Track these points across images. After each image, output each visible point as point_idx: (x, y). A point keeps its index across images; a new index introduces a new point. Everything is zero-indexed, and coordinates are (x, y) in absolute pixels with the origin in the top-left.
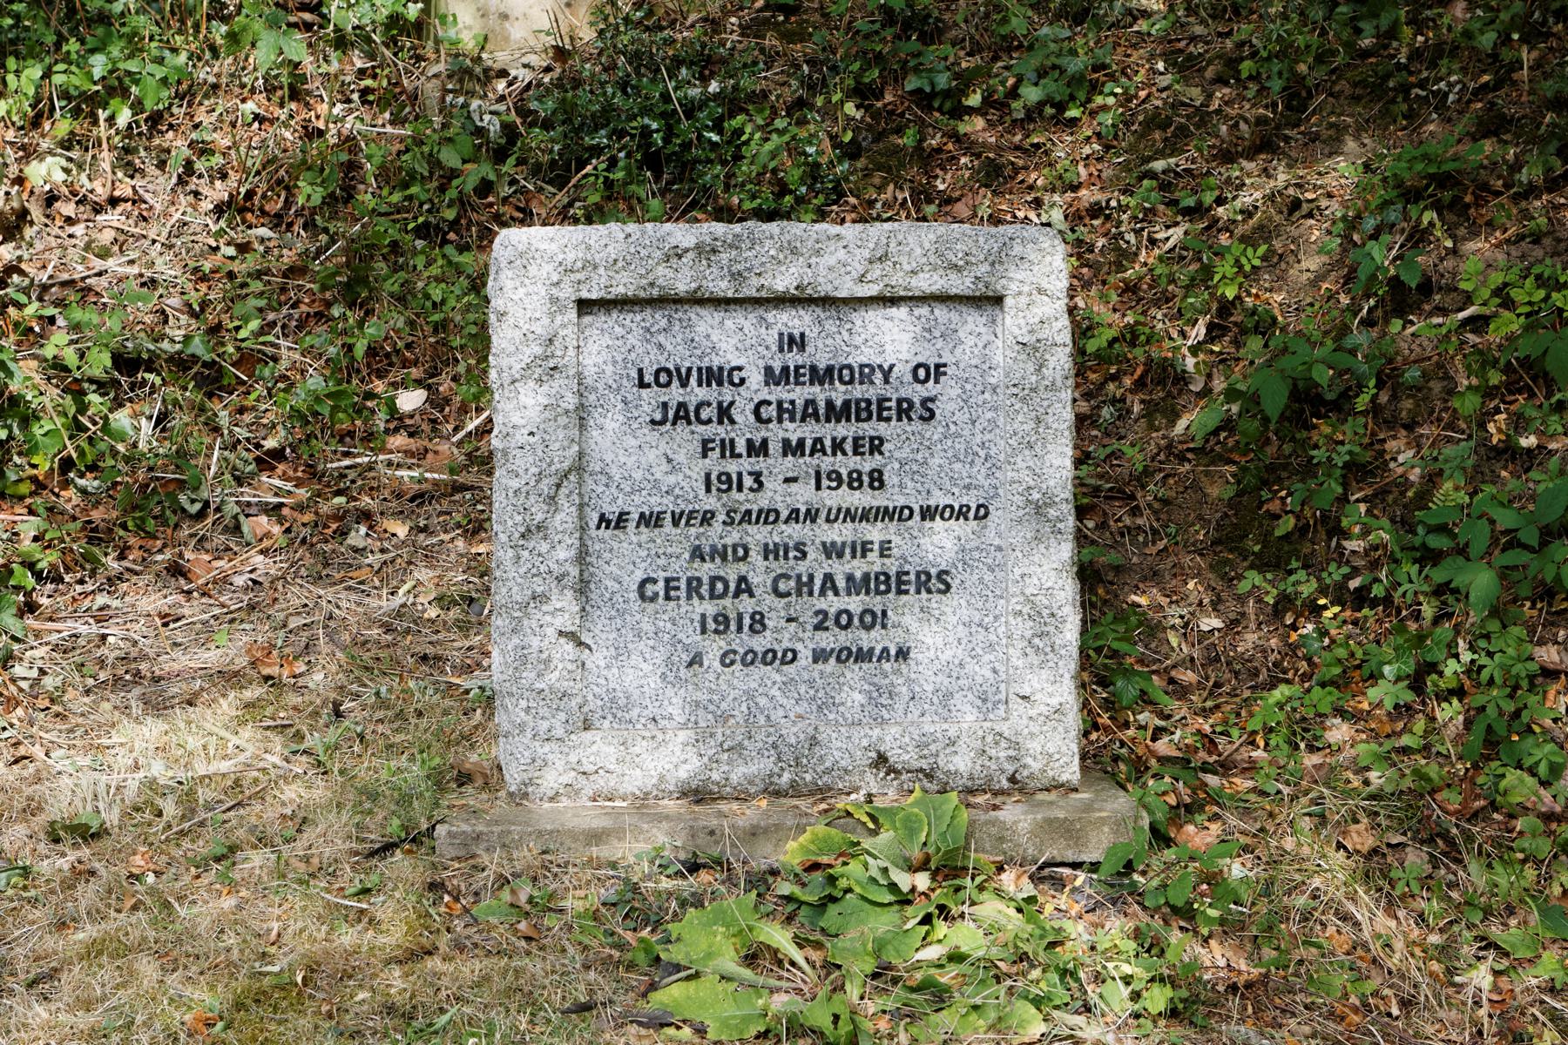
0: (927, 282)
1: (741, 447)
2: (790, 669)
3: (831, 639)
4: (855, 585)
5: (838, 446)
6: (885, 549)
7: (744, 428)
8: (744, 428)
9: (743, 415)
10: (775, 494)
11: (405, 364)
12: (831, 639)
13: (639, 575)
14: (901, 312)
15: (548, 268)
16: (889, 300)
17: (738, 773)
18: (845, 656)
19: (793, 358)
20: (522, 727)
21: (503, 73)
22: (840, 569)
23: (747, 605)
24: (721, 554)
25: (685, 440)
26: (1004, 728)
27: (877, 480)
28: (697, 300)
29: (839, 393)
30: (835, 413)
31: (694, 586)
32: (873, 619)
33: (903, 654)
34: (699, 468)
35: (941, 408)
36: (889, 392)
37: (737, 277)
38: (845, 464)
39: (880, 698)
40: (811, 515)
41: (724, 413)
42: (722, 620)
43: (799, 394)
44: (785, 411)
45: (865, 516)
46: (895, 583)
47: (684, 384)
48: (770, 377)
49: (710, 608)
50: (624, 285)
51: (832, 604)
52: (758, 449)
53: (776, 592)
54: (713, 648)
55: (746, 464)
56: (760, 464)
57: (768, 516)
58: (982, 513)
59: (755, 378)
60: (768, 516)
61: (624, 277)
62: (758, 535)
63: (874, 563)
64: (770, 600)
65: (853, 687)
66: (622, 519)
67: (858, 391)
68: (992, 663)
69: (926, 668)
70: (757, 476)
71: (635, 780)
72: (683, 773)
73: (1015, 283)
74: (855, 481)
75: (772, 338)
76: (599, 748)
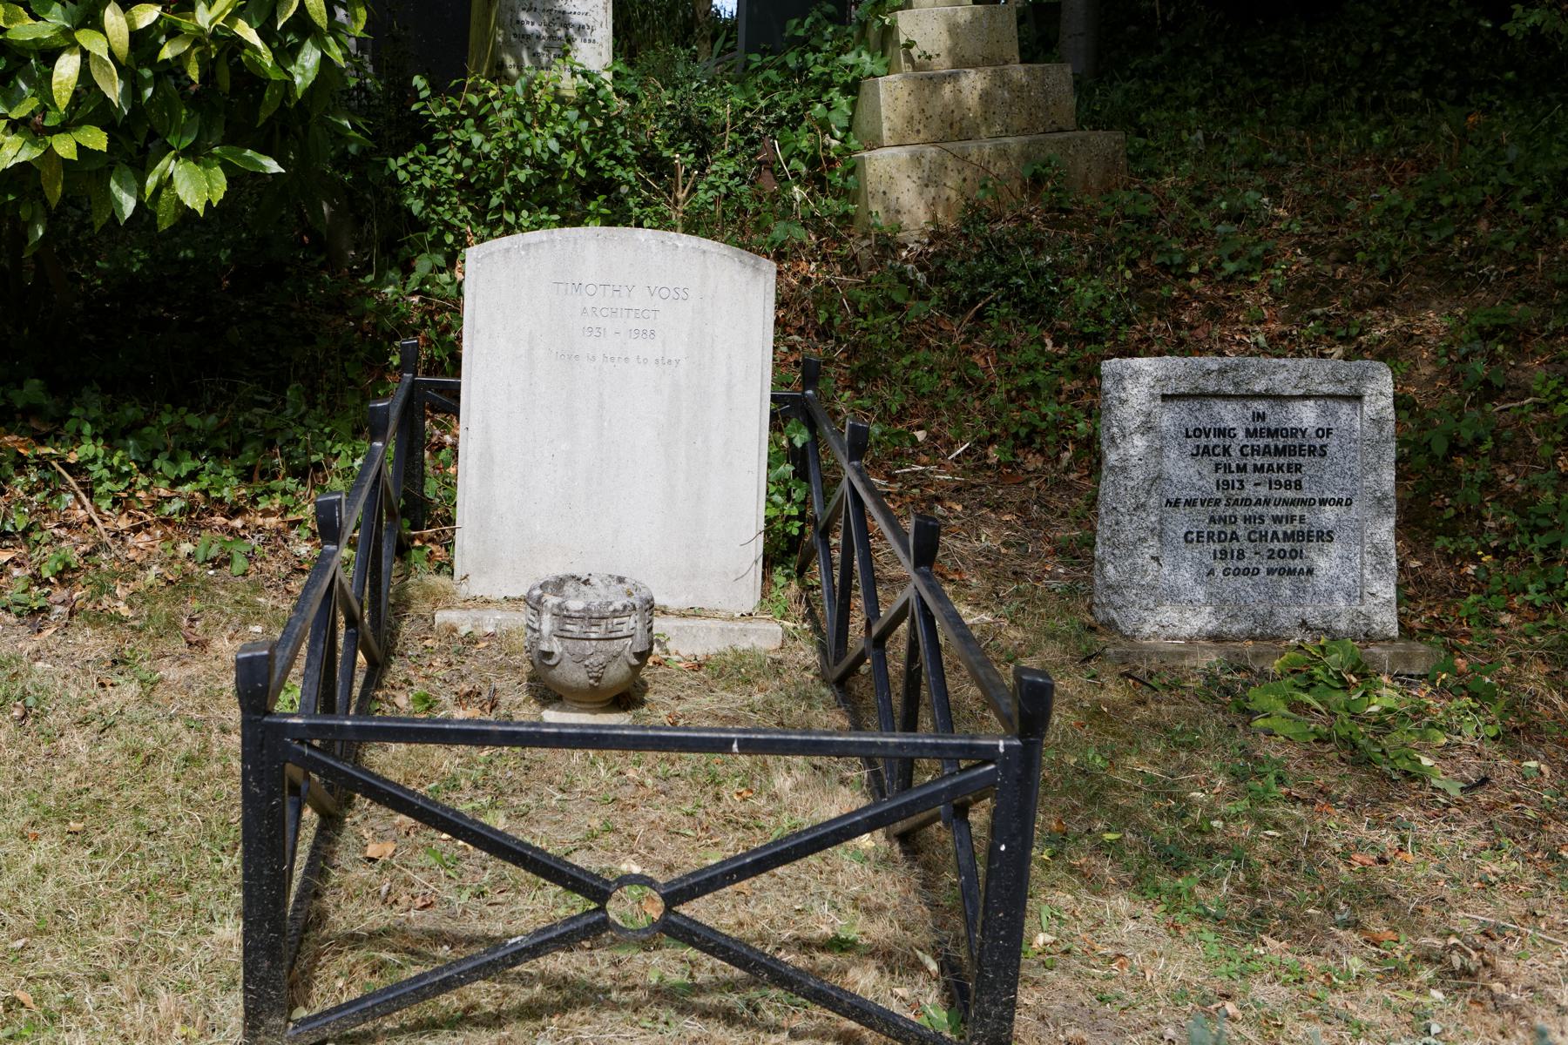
0: (1327, 388)
1: (1234, 468)
2: (1256, 578)
3: (1275, 563)
4: (1288, 537)
5: (1280, 468)
6: (1302, 519)
7: (1235, 459)
8: (1235, 459)
9: (1235, 452)
10: (1249, 491)
11: (913, 416)
12: (1275, 563)
13: (1185, 530)
14: (1311, 403)
15: (1148, 379)
16: (1305, 397)
17: (1235, 628)
18: (1283, 572)
19: (1259, 425)
20: (1133, 603)
21: (905, 246)
22: (1281, 529)
23: (1236, 546)
24: (1223, 520)
25: (1207, 464)
26: (1362, 608)
27: (1298, 485)
28: (1218, 395)
29: (1281, 442)
30: (1279, 452)
31: (1210, 536)
32: (1296, 554)
33: (1310, 571)
34: (1213, 478)
35: (1330, 450)
36: (1305, 442)
37: (1236, 384)
38: (1283, 477)
39: (1298, 592)
40: (1267, 502)
41: (1226, 451)
42: (1224, 552)
43: (1261, 442)
44: (1255, 450)
45: (1293, 503)
46: (1306, 536)
47: (1207, 436)
48: (1248, 433)
49: (1218, 547)
50: (1184, 388)
51: (1276, 546)
52: (1242, 469)
53: (1251, 541)
54: (1219, 567)
55: (1236, 476)
56: (1243, 476)
57: (1246, 502)
58: (1349, 503)
59: (1241, 434)
60: (1246, 502)
61: (1184, 384)
62: (1241, 511)
63: (1297, 525)
64: (1246, 543)
65: (1286, 586)
66: (1177, 501)
67: (1290, 441)
68: (1356, 576)
69: (1321, 582)
70: (1241, 482)
71: (1186, 630)
72: (1209, 627)
73: (1369, 389)
74: (1288, 485)
75: (1249, 414)
76: (1168, 614)
